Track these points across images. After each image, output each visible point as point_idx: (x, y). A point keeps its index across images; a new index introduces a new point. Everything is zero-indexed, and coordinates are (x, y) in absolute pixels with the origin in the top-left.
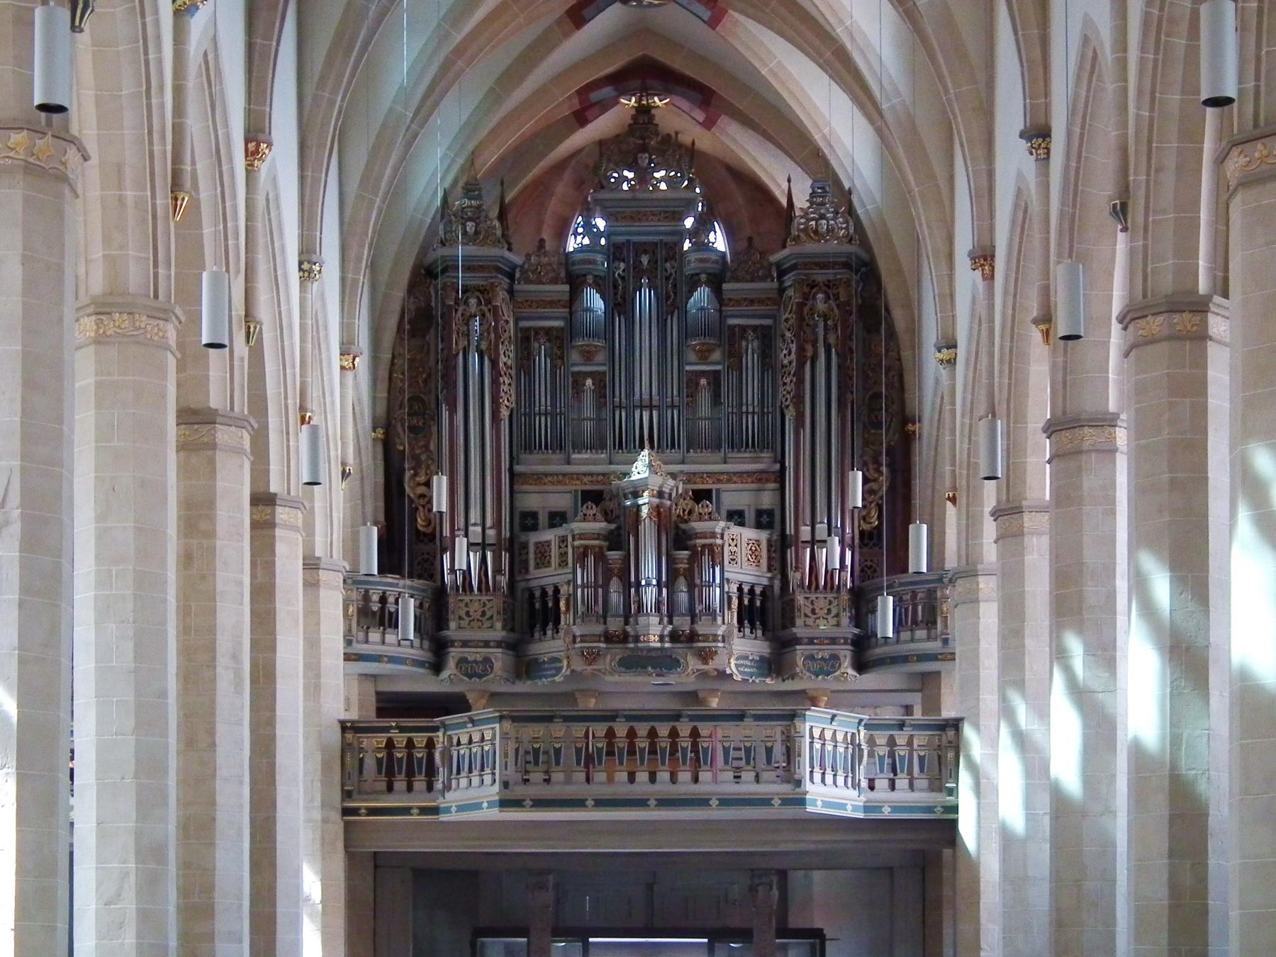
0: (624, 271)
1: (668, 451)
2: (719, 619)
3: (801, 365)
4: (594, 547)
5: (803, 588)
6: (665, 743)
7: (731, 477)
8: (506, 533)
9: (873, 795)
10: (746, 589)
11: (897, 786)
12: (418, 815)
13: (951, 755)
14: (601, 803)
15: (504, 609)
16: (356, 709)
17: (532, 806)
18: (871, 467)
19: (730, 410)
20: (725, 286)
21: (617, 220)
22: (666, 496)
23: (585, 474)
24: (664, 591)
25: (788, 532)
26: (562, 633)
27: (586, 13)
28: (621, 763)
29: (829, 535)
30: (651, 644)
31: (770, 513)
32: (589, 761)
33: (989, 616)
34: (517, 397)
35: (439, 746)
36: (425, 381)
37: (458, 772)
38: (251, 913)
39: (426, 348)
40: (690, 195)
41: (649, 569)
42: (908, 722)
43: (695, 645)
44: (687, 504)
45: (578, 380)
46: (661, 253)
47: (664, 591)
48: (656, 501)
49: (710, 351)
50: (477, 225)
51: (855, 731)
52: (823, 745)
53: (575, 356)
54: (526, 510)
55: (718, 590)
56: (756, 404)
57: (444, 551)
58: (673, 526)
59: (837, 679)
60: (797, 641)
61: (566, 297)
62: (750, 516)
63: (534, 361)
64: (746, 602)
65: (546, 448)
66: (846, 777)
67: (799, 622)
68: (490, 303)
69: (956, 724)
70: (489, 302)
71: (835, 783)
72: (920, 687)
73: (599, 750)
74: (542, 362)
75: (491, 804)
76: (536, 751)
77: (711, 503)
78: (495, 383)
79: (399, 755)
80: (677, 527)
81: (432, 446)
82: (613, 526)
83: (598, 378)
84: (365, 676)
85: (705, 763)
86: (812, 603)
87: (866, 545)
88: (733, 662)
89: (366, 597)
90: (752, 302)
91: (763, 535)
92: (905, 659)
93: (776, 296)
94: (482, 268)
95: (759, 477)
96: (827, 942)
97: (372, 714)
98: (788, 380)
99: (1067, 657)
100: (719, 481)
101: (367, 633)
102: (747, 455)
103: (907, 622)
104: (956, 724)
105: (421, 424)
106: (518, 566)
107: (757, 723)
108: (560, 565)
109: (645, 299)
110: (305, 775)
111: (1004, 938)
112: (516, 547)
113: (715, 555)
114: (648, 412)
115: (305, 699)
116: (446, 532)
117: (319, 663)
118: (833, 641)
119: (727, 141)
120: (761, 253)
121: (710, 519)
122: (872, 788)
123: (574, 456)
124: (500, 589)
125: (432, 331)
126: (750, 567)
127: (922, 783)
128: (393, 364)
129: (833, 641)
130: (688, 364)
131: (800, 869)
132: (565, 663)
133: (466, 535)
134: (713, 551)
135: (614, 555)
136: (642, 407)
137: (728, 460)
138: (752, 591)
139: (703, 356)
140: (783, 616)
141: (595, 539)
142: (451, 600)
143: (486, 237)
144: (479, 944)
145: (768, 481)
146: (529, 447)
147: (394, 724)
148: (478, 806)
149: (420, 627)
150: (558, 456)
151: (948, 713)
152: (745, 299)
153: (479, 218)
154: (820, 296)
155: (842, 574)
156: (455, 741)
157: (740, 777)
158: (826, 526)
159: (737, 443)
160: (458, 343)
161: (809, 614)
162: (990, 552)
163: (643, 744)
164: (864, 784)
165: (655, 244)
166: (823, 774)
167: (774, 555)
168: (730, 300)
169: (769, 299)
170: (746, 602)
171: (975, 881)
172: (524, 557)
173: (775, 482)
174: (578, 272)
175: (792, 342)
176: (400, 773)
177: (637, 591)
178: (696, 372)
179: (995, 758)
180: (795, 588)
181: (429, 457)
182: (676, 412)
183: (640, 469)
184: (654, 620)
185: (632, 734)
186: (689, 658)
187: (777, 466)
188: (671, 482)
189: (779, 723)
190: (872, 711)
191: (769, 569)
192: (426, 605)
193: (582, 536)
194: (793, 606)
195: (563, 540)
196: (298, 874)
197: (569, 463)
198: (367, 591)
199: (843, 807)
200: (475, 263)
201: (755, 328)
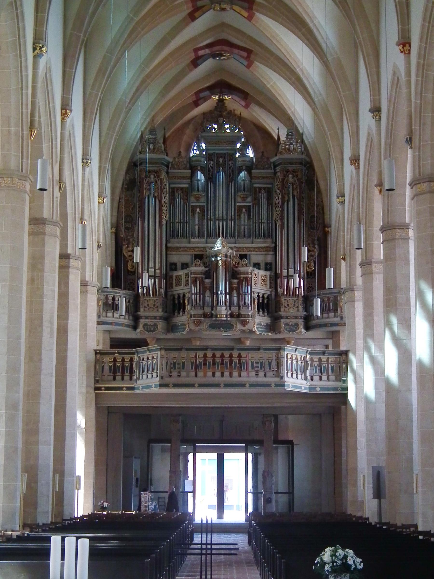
1: (230, 238)
2: (250, 308)
4: (199, 277)
5: (284, 295)
6: (227, 360)
7: (255, 249)
8: (164, 272)
9: (312, 383)
10: (261, 296)
11: (322, 379)
12: (126, 390)
13: (344, 366)
14: (201, 386)
15: (163, 303)
16: (102, 345)
17: (173, 387)
18: (311, 245)
19: (255, 221)
20: (253, 171)
21: (210, 144)
22: (229, 256)
23: (196, 248)
24: (228, 296)
25: (278, 272)
26: (186, 313)
28: (209, 368)
29: (295, 273)
30: (223, 319)
31: (271, 264)
32: (196, 367)
33: (359, 307)
34: (169, 216)
35: (135, 361)
36: (132, 209)
37: (143, 372)
38: (55, 433)
40: (239, 135)
41: (222, 287)
42: (326, 351)
43: (240, 319)
44: (237, 260)
45: (194, 209)
47: (228, 296)
48: (225, 259)
49: (247, 197)
50: (154, 146)
52: (292, 361)
53: (193, 199)
54: (173, 262)
55: (249, 296)
56: (265, 219)
57: (139, 279)
58: (231, 269)
59: (298, 333)
60: (281, 317)
61: (189, 175)
62: (262, 265)
63: (176, 201)
64: (261, 301)
65: (181, 236)
66: (302, 375)
67: (282, 309)
69: (346, 353)
70: (158, 177)
71: (297, 377)
72: (331, 337)
73: (201, 363)
74: (179, 201)
75: (156, 386)
76: (175, 363)
77: (247, 259)
78: (160, 210)
79: (119, 365)
80: (233, 269)
81: (135, 236)
82: (207, 269)
84: (105, 331)
85: (244, 369)
86: (288, 301)
87: (310, 278)
88: (255, 325)
89: (107, 298)
90: (263, 178)
91: (268, 273)
92: (325, 325)
93: (273, 175)
94: (156, 163)
95: (266, 249)
96: (294, 446)
97: (108, 347)
98: (278, 210)
99: (391, 324)
100: (250, 251)
101: (107, 313)
102: (262, 240)
103: (326, 310)
104: (346, 353)
105: (130, 226)
106: (169, 286)
107: (266, 352)
108: (185, 285)
109: (221, 176)
110: (79, 373)
111: (367, 444)
112: (168, 277)
113: (248, 281)
114: (222, 222)
115: (80, 340)
116: (140, 271)
117: (86, 325)
118: (296, 317)
119: (254, 113)
120: (267, 158)
121: (247, 266)
122: (312, 379)
123: (192, 240)
124: (161, 295)
125: (135, 188)
127: (332, 378)
128: (119, 202)
129: (296, 317)
130: (238, 202)
131: (284, 414)
132: (187, 326)
133: (148, 272)
134: (248, 279)
135: (207, 281)
136: (219, 220)
137: (254, 242)
138: (263, 297)
139: (244, 199)
140: (276, 307)
142: (141, 299)
143: (158, 151)
144: (150, 446)
145: (270, 251)
146: (173, 236)
147: (117, 351)
148: (150, 387)
149: (128, 310)
150: (185, 240)
151: (343, 348)
152: (261, 177)
153: (155, 143)
154: (290, 176)
155: (300, 289)
156: (141, 359)
157: (258, 375)
158: (293, 269)
160: (146, 193)
161: (286, 306)
162: (359, 281)
163: (218, 360)
164: (309, 378)
165: (225, 154)
166: (292, 374)
167: (272, 282)
168: (255, 177)
169: (270, 176)
170: (261, 301)
171: (355, 420)
172: (171, 282)
173: (273, 251)
175: (280, 194)
176: (119, 372)
177: (217, 296)
179: (363, 366)
180: (281, 295)
181: (133, 240)
182: (233, 222)
183: (218, 245)
184: (224, 308)
185: (214, 356)
186: (238, 324)
187: (274, 245)
188: (231, 251)
189: (274, 352)
190: (312, 347)
191: (270, 287)
192: (131, 301)
193: (195, 273)
194: (280, 303)
195: (187, 274)
196: (75, 416)
197: (189, 243)
198: (107, 295)
199: (300, 388)
201: (265, 188)
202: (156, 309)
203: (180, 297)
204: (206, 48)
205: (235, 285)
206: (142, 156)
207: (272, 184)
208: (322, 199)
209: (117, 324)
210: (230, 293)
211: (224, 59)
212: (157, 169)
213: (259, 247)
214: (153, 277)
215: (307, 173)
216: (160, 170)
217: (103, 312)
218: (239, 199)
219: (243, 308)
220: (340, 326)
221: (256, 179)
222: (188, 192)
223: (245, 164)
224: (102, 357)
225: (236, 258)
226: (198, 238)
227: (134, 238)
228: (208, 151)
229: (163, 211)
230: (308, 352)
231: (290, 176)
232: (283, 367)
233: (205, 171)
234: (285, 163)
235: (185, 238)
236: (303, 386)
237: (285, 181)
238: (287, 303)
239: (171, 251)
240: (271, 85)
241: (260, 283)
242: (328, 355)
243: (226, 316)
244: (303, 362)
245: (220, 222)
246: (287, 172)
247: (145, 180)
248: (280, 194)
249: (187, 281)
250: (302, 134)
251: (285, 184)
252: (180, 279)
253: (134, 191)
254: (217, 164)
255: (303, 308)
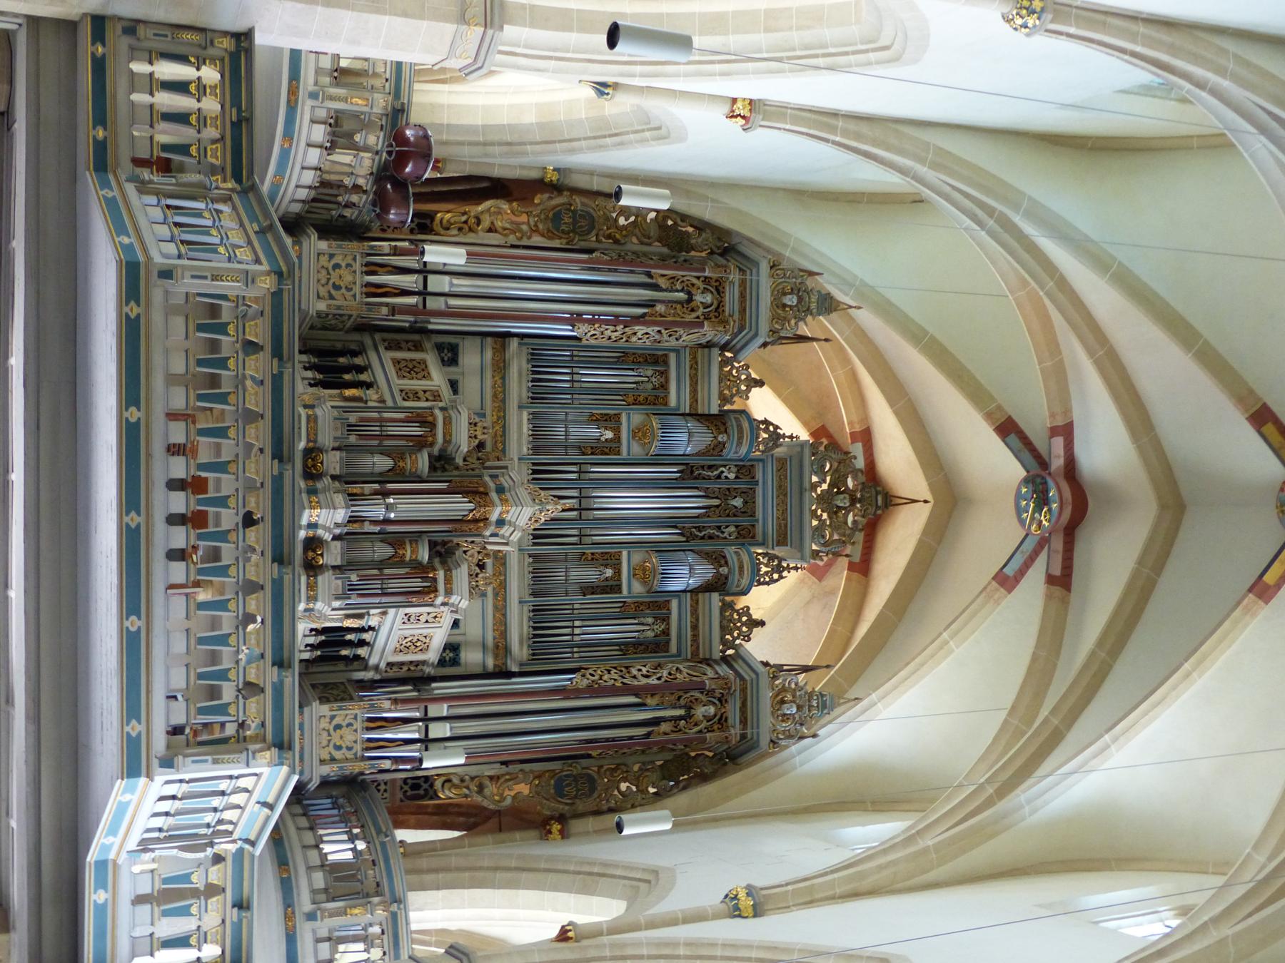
0: (726, 477)
2: (337, 604)
3: (635, 691)
8: (437, 324)
10: (367, 636)
19: (576, 606)
20: (715, 597)
22: (497, 530)
23: (504, 427)
24: (377, 529)
25: (434, 685)
27: (1013, 438)
30: (306, 513)
31: (455, 662)
39: (646, 240)
42: (249, 914)
44: (472, 556)
45: (610, 421)
46: (744, 521)
47: (377, 529)
49: (644, 581)
51: (235, 836)
53: (637, 418)
58: (445, 539)
63: (632, 369)
67: (325, 709)
68: (705, 318)
70: (707, 317)
74: (628, 378)
82: (459, 461)
83: (611, 448)
86: (350, 725)
90: (695, 627)
91: (432, 656)
93: (701, 656)
95: (501, 648)
98: (614, 674)
100: (496, 595)
105: (563, 227)
108: (401, 391)
112: (416, 337)
124: (370, 310)
126: (396, 639)
130: (629, 552)
134: (429, 593)
135: (423, 462)
136: (580, 498)
138: (362, 643)
139: (641, 573)
140: (326, 685)
141: (444, 436)
142: (354, 247)
145: (496, 656)
146: (534, 357)
150: (525, 394)
159: (541, 616)
161: (335, 722)
165: (753, 515)
167: (405, 668)
168: (697, 601)
169: (698, 648)
170: (349, 637)
172: (403, 345)
173: (495, 666)
174: (729, 424)
175: (659, 679)
177: (376, 493)
178: (620, 564)
181: (523, 234)
184: (340, 515)
187: (515, 669)
191: (390, 665)
192: (347, 213)
193: (448, 422)
194: (342, 700)
195: (436, 396)
197: (520, 407)
199: (113, 831)
200: (748, 303)
201: (666, 633)
202: (323, 292)
203: (362, 373)
204: (1066, 460)
205: (412, 552)
206: (764, 267)
207: (679, 654)
208: (640, 805)
209: (285, 154)
210: (385, 538)
211: (1019, 511)
212: (727, 314)
213: (506, 624)
214: (421, 287)
215: (707, 756)
216: (724, 322)
217: (329, 109)
218: (637, 557)
219: (339, 582)
220: (286, 914)
221: (691, 606)
222: (654, 404)
223: (734, 574)
224: (222, 60)
225: (479, 552)
226: (531, 433)
227: (529, 238)
228: (761, 464)
229: (612, 328)
230: (247, 847)
231: (712, 710)
232: (209, 765)
233: (712, 455)
234: (744, 690)
235: (531, 395)
236: (118, 840)
237: (697, 694)
238: (344, 724)
239: (493, 348)
240: (947, 643)
241: (407, 633)
242: (235, 919)
243: (313, 526)
244: (211, 830)
245: (574, 501)
246: (720, 700)
247: (698, 278)
248: (659, 679)
249: (416, 396)
250: (814, 736)
251: (688, 695)
252: (417, 373)
253: (657, 244)
254: (728, 489)
255: (328, 774)
